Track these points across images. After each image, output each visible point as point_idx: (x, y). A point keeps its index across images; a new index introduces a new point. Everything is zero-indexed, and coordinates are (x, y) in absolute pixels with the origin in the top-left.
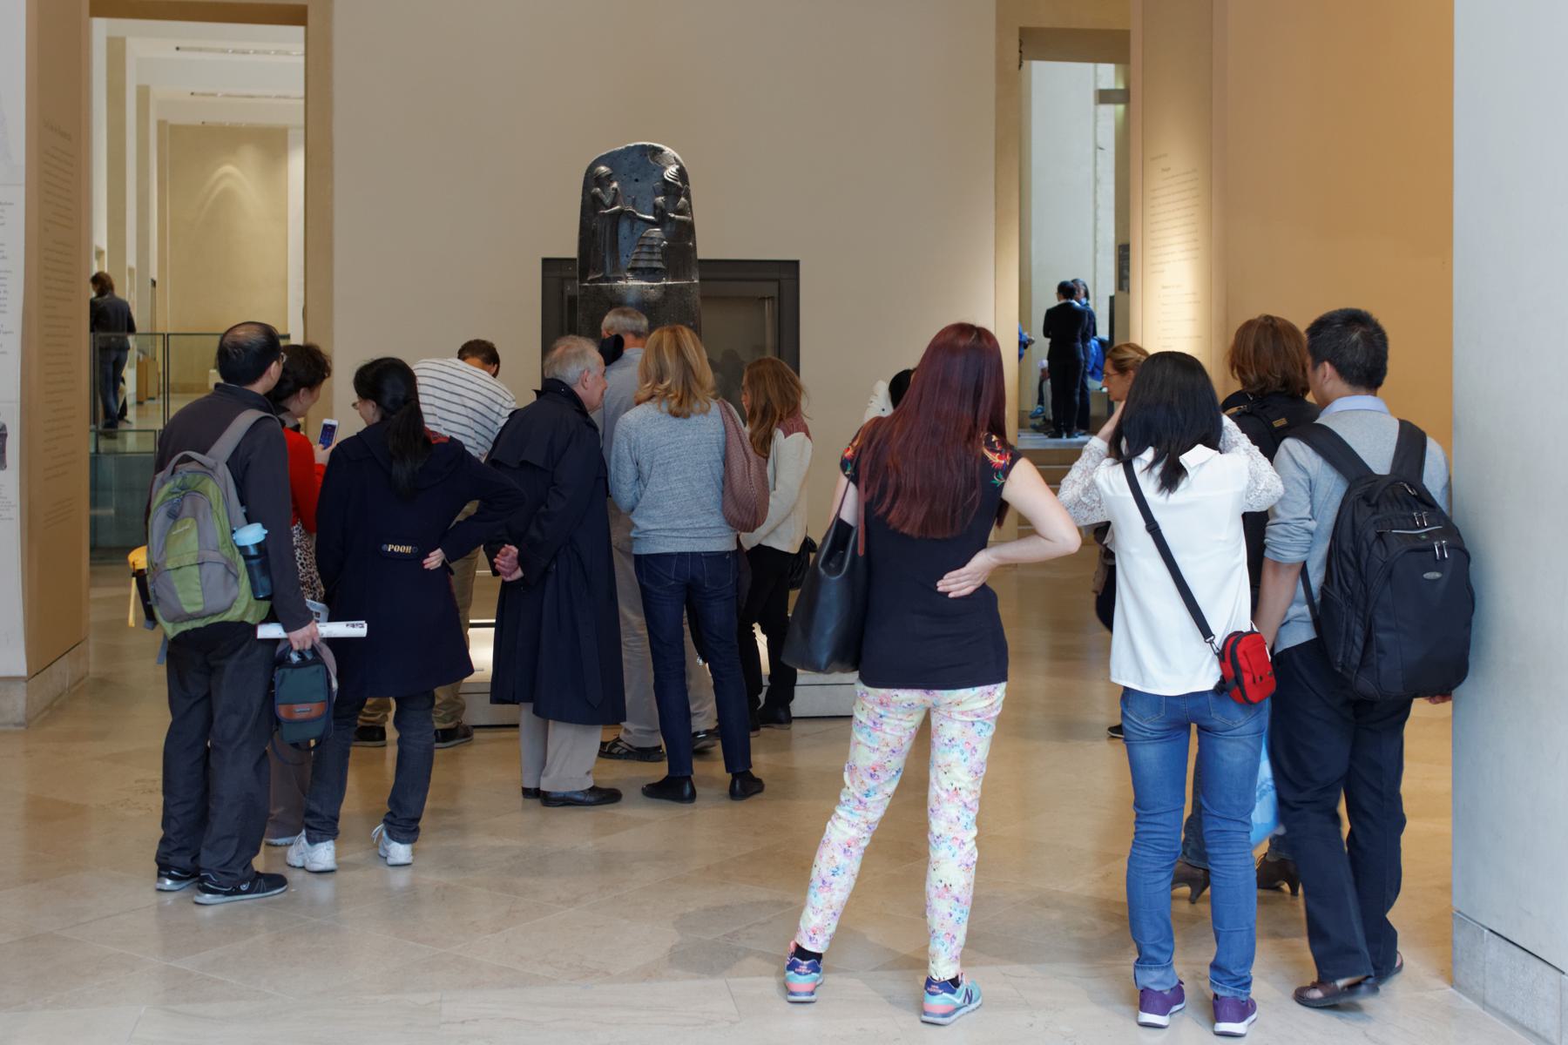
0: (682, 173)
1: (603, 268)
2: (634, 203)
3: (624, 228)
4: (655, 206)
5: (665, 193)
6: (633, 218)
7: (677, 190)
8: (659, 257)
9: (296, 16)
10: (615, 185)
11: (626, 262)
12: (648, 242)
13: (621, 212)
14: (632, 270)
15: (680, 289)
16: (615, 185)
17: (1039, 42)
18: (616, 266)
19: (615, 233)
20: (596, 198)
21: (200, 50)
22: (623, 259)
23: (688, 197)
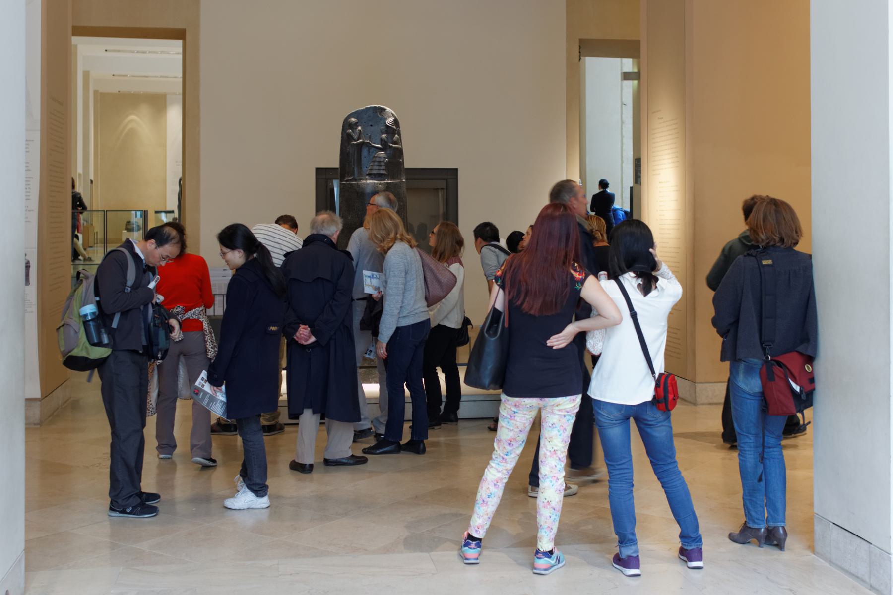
0: (396, 122)
1: (353, 174)
2: (370, 138)
3: (365, 152)
4: (381, 140)
5: (387, 132)
6: (369, 146)
7: (393, 131)
9: (179, 34)
10: (360, 128)
11: (366, 170)
12: (377, 159)
13: (363, 143)
14: (369, 175)
15: (396, 184)
16: (360, 128)
17: (590, 47)
18: (360, 174)
20: (349, 135)
21: (119, 51)
22: (364, 169)
23: (399, 135)
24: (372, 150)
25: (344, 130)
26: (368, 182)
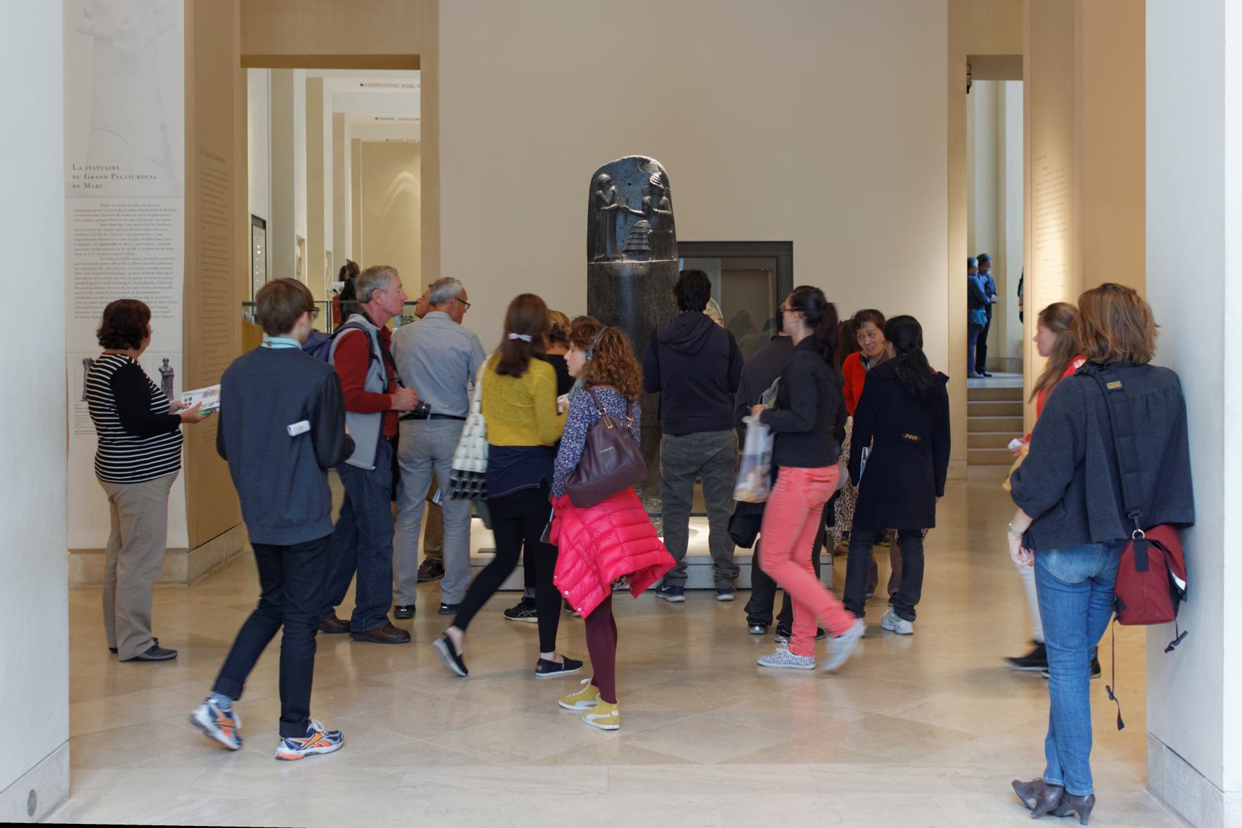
0: (664, 178)
1: (604, 251)
2: (627, 201)
3: (620, 219)
4: (644, 204)
6: (627, 213)
7: (660, 191)
8: (645, 241)
9: (411, 63)
13: (618, 208)
14: (627, 251)
15: (664, 265)
16: (613, 188)
17: (978, 66)
18: (614, 250)
19: (614, 224)
20: (599, 198)
21: (378, 85)
22: (620, 244)
23: (668, 196)
24: (631, 218)
25: (592, 191)
26: (625, 262)
